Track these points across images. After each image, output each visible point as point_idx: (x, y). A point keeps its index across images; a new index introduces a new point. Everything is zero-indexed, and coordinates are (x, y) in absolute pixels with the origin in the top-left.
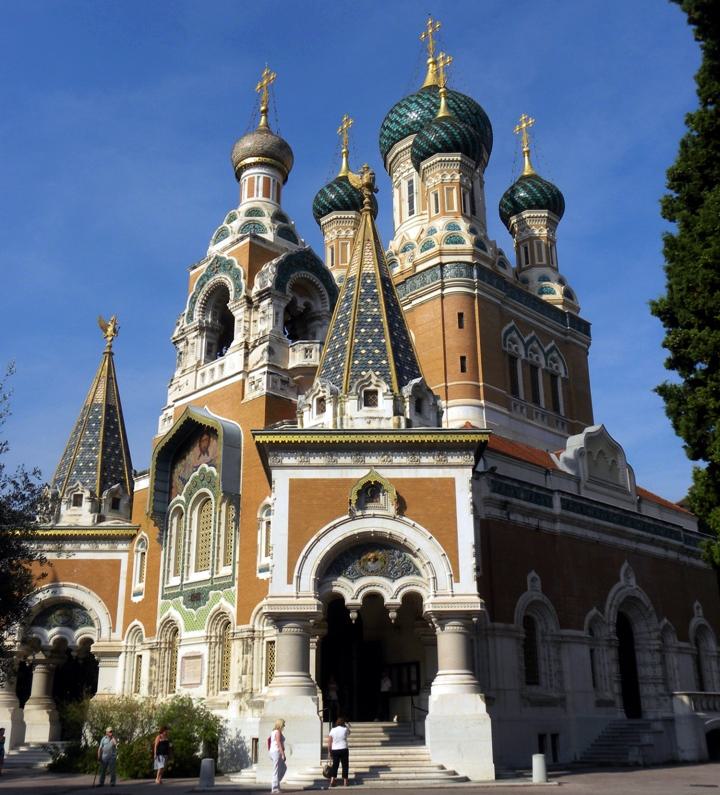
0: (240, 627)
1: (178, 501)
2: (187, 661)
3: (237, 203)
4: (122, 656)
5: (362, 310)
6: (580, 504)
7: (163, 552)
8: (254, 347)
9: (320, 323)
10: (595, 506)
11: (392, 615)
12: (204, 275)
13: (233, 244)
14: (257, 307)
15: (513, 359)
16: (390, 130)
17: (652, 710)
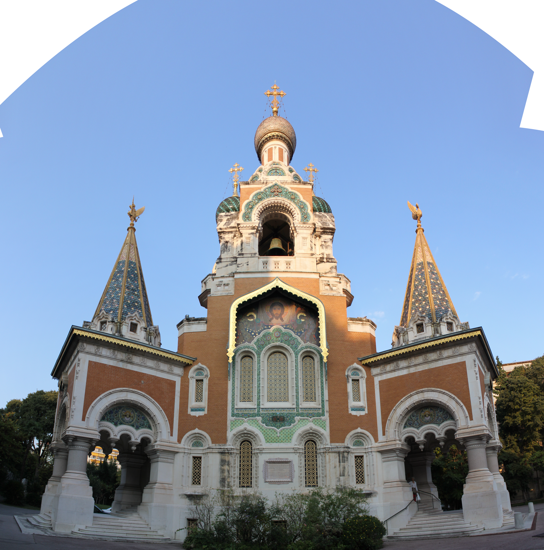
0: (337, 444)
2: (269, 464)
4: (178, 457)
7: (230, 383)
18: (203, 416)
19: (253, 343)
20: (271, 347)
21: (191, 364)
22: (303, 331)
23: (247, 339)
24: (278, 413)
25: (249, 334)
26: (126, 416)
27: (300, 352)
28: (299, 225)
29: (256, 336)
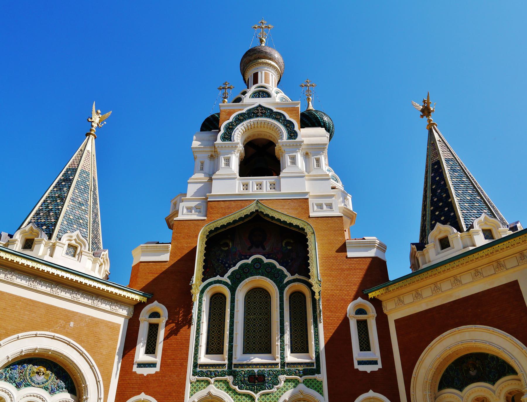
12: (244, 114)
18: (154, 374)
19: (226, 275)
20: (249, 282)
22: (289, 261)
23: (219, 271)
24: (256, 370)
25: (222, 265)
26: (38, 373)
27: (286, 287)
29: (230, 269)
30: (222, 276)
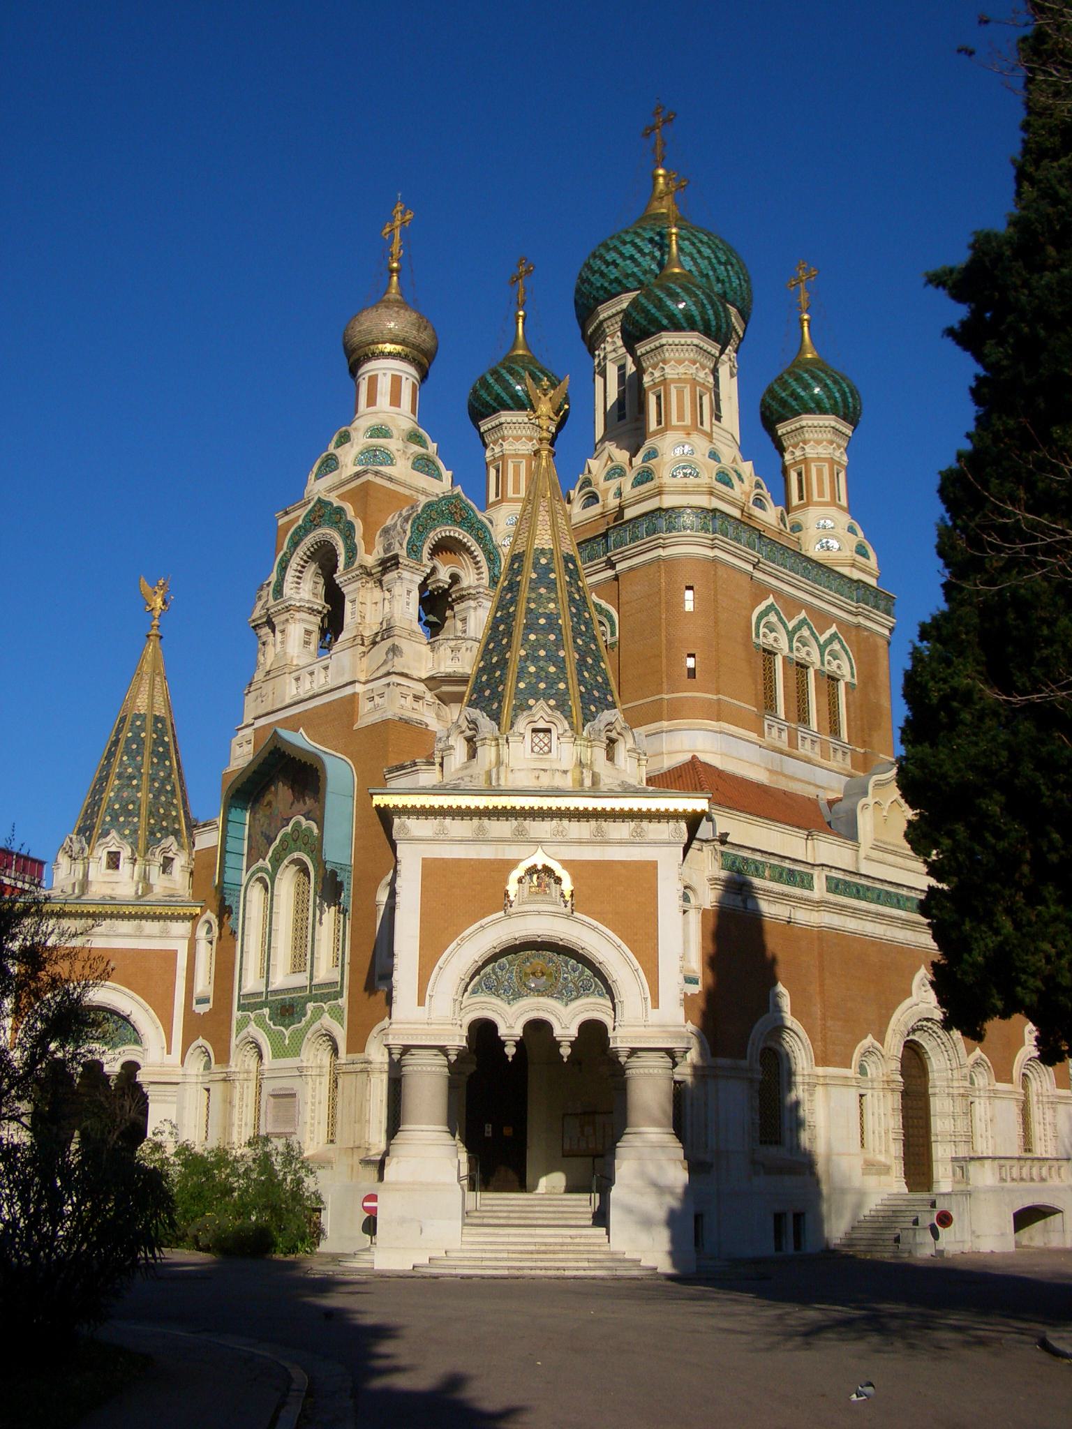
0: (351, 1056)
1: (261, 869)
3: (352, 411)
5: (532, 606)
6: (856, 885)
8: (374, 643)
9: (472, 603)
10: (878, 886)
11: (565, 1051)
12: (300, 527)
13: (343, 484)
14: (380, 582)
15: (769, 653)
16: (591, 284)
17: (944, 1178)
19: (267, 860)
21: (197, 915)
28: (341, 580)
30: (264, 860)
